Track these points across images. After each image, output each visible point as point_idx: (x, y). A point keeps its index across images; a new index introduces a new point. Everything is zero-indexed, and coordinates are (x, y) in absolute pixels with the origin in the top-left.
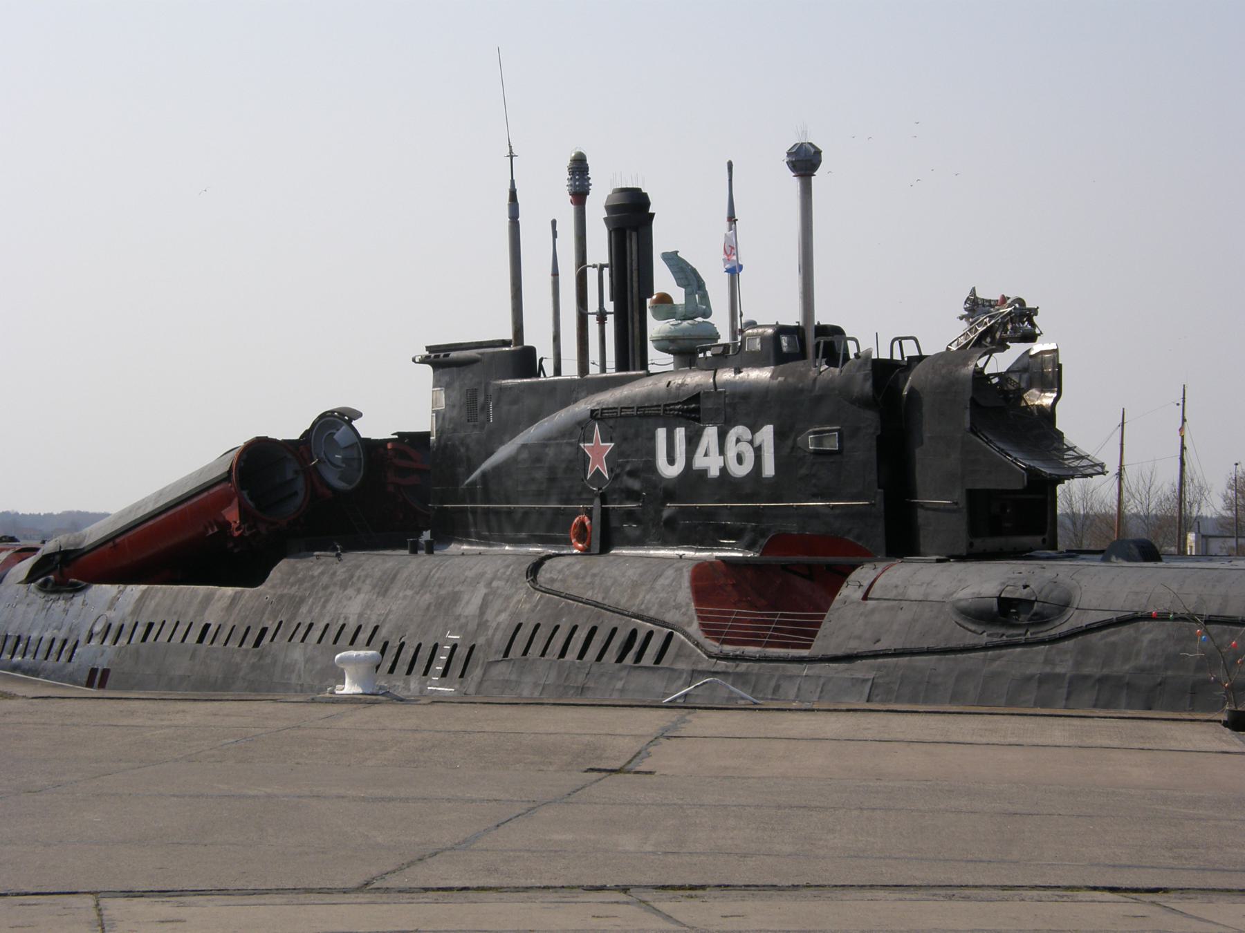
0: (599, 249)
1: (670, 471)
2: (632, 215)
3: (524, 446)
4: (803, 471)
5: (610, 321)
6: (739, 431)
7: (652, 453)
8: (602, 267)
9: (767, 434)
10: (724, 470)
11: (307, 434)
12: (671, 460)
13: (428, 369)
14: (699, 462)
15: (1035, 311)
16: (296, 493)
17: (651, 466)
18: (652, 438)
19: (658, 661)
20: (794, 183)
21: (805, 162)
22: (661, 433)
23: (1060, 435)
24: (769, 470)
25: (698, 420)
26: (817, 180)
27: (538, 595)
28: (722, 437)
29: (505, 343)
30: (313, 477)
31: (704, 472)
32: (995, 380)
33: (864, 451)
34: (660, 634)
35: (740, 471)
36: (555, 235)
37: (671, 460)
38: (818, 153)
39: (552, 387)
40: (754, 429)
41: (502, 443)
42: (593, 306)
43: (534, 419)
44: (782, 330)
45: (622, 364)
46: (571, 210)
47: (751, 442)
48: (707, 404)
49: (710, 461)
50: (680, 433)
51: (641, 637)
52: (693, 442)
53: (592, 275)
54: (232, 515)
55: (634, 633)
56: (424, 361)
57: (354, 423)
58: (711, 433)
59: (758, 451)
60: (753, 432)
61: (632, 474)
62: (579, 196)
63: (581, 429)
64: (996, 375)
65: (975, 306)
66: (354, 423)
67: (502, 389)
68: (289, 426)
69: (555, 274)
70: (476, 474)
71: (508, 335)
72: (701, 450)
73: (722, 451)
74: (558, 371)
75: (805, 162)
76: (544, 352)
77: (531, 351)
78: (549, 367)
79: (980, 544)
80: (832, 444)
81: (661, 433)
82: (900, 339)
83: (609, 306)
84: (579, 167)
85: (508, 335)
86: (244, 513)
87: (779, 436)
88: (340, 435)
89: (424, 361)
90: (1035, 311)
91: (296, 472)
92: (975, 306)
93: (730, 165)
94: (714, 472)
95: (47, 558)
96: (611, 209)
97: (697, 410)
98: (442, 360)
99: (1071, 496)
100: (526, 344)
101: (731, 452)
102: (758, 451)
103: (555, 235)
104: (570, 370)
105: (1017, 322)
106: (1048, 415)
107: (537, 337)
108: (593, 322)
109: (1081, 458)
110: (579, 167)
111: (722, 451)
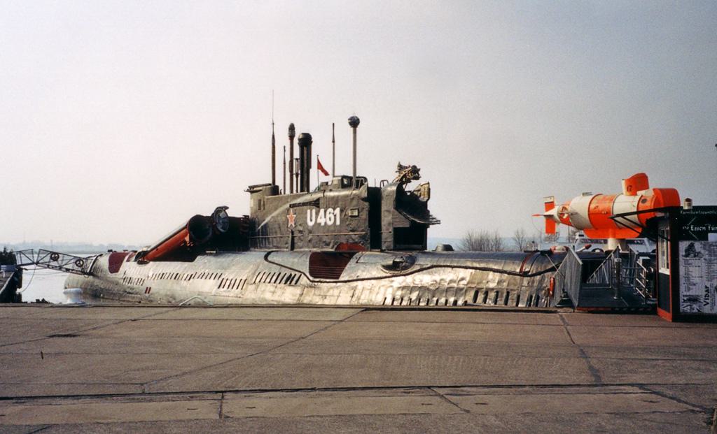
0: (297, 155)
1: (311, 224)
2: (306, 141)
3: (272, 217)
4: (347, 223)
5: (299, 176)
6: (330, 210)
7: (306, 218)
8: (297, 159)
9: (338, 211)
10: (326, 223)
11: (213, 214)
12: (311, 220)
13: (249, 193)
14: (319, 221)
15: (419, 170)
16: (209, 233)
17: (307, 224)
18: (306, 213)
19: (296, 284)
20: (352, 129)
21: (354, 123)
22: (309, 211)
23: (429, 211)
24: (338, 223)
25: (319, 207)
26: (358, 129)
27: (266, 263)
28: (325, 212)
29: (270, 185)
30: (215, 227)
31: (320, 224)
32: (409, 194)
33: (365, 215)
34: (298, 274)
35: (330, 223)
36: (285, 151)
37: (311, 220)
38: (358, 120)
39: (281, 198)
40: (334, 209)
41: (267, 216)
42: (294, 172)
44: (344, 177)
45: (302, 191)
46: (289, 141)
48: (321, 202)
49: (322, 221)
50: (314, 211)
51: (293, 276)
52: (317, 214)
53: (294, 161)
54: (187, 239)
55: (291, 275)
56: (248, 191)
57: (226, 211)
58: (322, 211)
59: (335, 216)
60: (334, 209)
61: (300, 225)
62: (292, 137)
63: (288, 210)
64: (410, 192)
65: (401, 167)
66: (226, 211)
67: (268, 199)
68: (207, 212)
69: (285, 163)
70: (260, 227)
71: (271, 182)
72: (319, 217)
73: (325, 217)
74: (285, 193)
75: (354, 123)
76: (281, 187)
77: (278, 187)
78: (282, 192)
79: (398, 246)
80: (356, 213)
81: (309, 211)
82: (383, 181)
83: (299, 173)
84: (292, 128)
85: (271, 182)
86: (191, 239)
87: (341, 211)
88: (222, 215)
89: (248, 191)
90: (419, 170)
91: (209, 227)
92: (401, 167)
93: (333, 124)
94: (323, 224)
95: (140, 253)
96: (300, 140)
97: (319, 204)
98: (252, 190)
99: (432, 232)
100: (276, 184)
101: (328, 218)
102: (335, 216)
103: (285, 151)
104: (288, 192)
105: (415, 173)
106: (425, 204)
107: (279, 183)
108: (294, 176)
109: (433, 219)
110: (292, 128)
111: (325, 217)
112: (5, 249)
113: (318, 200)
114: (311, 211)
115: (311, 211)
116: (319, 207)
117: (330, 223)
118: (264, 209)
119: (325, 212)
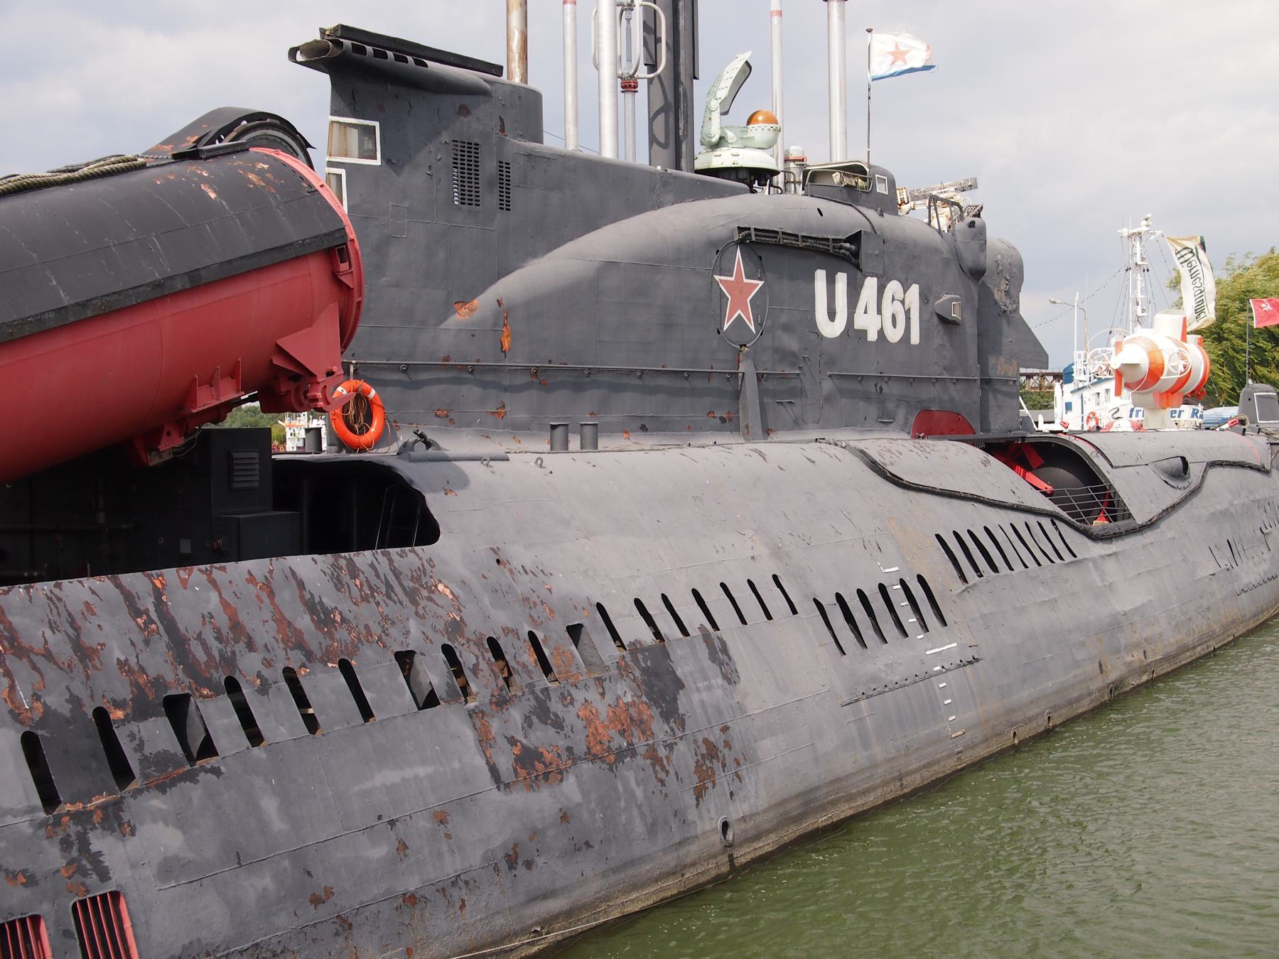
10: (881, 333)
12: (832, 315)
13: (321, 82)
18: (812, 279)
22: (821, 275)
24: (915, 339)
28: (881, 290)
31: (864, 332)
35: (894, 335)
37: (832, 315)
43: (591, 224)
47: (903, 302)
49: (868, 322)
50: (842, 279)
58: (871, 284)
59: (908, 313)
60: (905, 292)
61: (787, 328)
73: (879, 311)
87: (924, 298)
94: (872, 336)
97: (856, 254)
102: (908, 313)
111: (879, 311)
112: (1149, 354)
113: (856, 238)
114: (831, 282)
115: (831, 282)
116: (858, 267)
117: (894, 335)
118: (505, 205)
119: (881, 290)
